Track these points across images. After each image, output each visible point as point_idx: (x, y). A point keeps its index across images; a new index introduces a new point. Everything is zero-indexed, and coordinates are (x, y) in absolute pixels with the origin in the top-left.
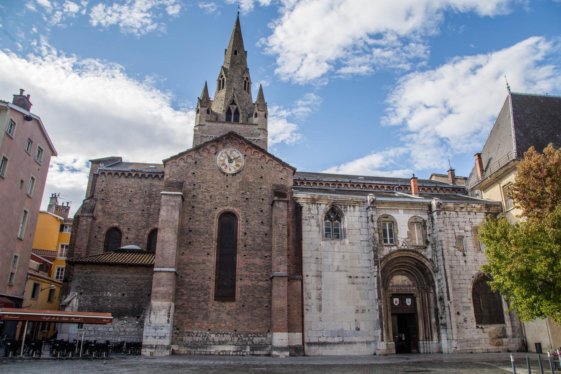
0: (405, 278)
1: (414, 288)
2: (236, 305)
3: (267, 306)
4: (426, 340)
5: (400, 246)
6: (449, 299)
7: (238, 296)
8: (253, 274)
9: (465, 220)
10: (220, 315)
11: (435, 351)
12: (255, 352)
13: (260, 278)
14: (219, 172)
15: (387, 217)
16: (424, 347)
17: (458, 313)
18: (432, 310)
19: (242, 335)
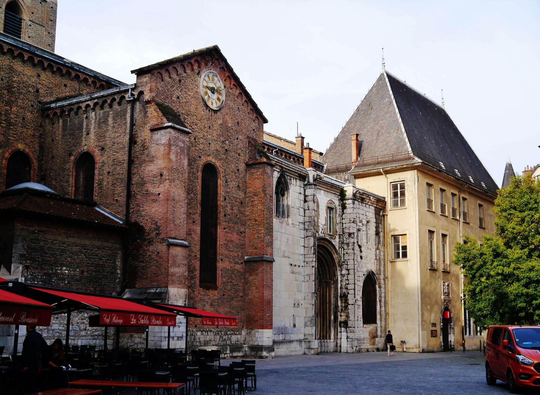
2: (218, 293)
3: (242, 296)
4: (323, 339)
5: (320, 233)
7: (220, 281)
8: (231, 253)
10: (204, 306)
11: (332, 350)
12: (235, 354)
13: (237, 260)
14: (202, 103)
18: (332, 307)
19: (223, 333)
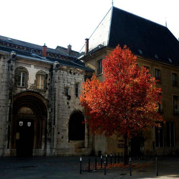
0: (29, 109)
1: (34, 116)
5: (28, 88)
6: (54, 124)
9: (72, 78)
15: (23, 68)
16: (35, 153)
17: (59, 133)
18: (44, 130)
